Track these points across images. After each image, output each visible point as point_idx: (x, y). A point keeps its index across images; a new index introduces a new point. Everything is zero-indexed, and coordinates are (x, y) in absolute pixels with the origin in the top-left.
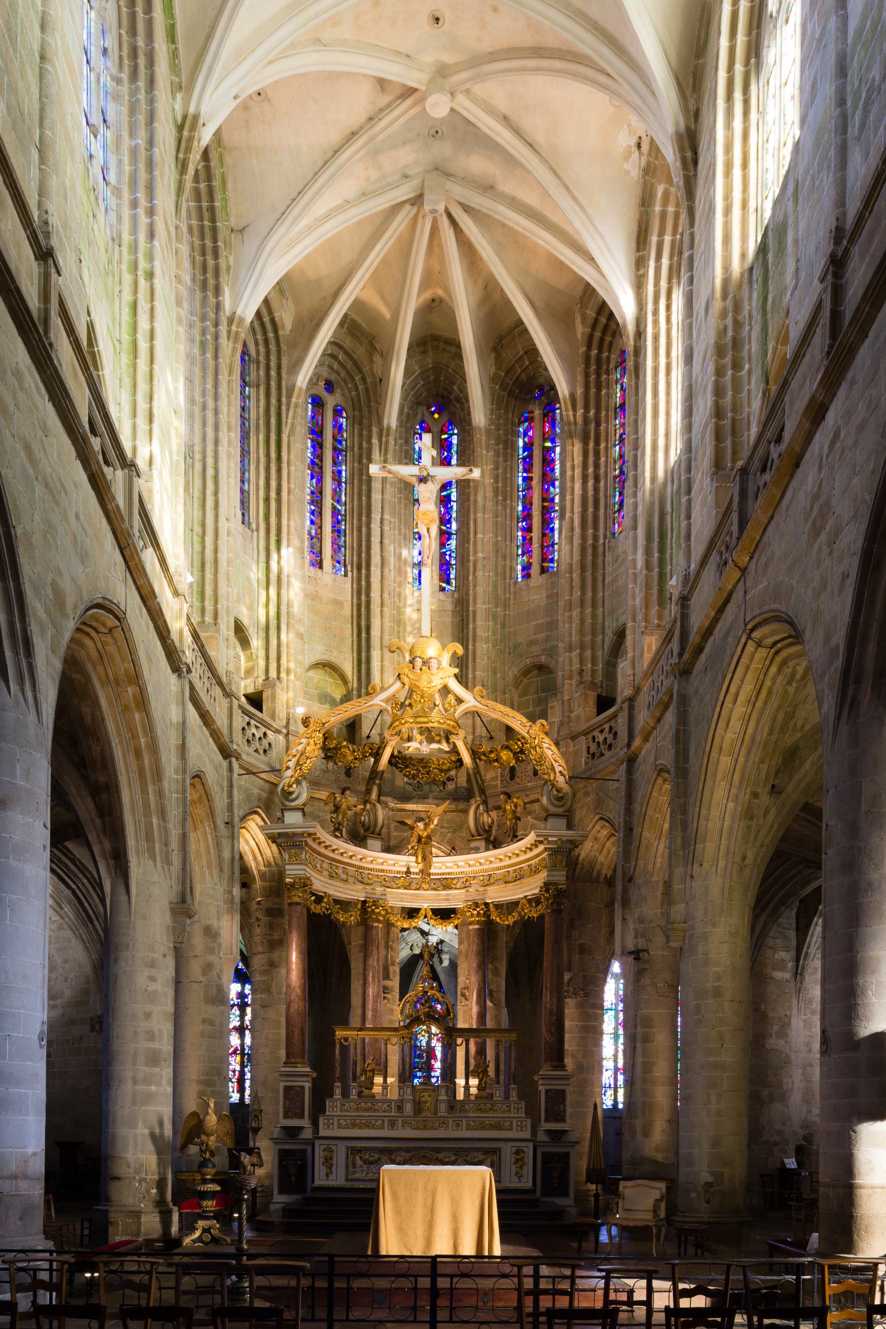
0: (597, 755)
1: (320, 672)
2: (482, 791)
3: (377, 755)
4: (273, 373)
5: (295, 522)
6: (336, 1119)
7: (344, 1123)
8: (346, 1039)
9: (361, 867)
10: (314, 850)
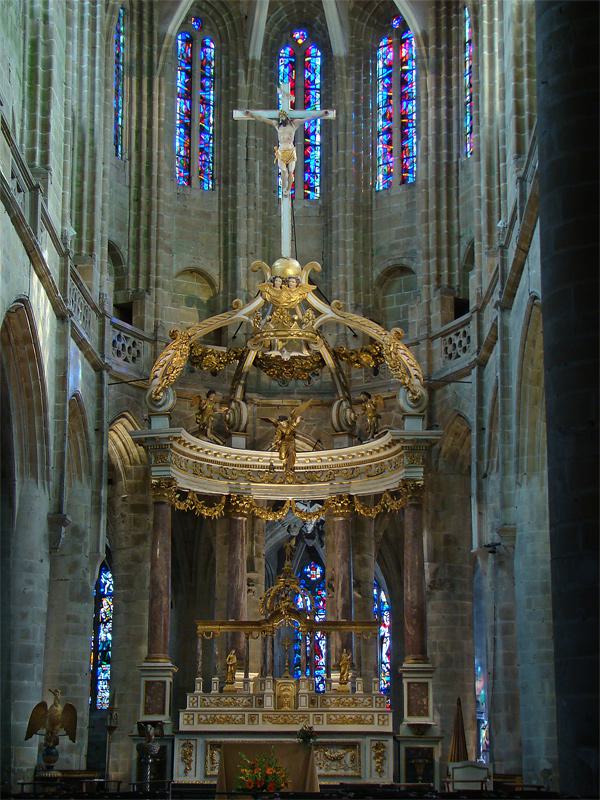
0: (454, 356)
1: (188, 277)
2: (345, 388)
3: (242, 358)
4: (146, 23)
5: (165, 150)
6: (196, 715)
7: (204, 718)
8: (208, 634)
9: (225, 464)
10: (179, 452)
